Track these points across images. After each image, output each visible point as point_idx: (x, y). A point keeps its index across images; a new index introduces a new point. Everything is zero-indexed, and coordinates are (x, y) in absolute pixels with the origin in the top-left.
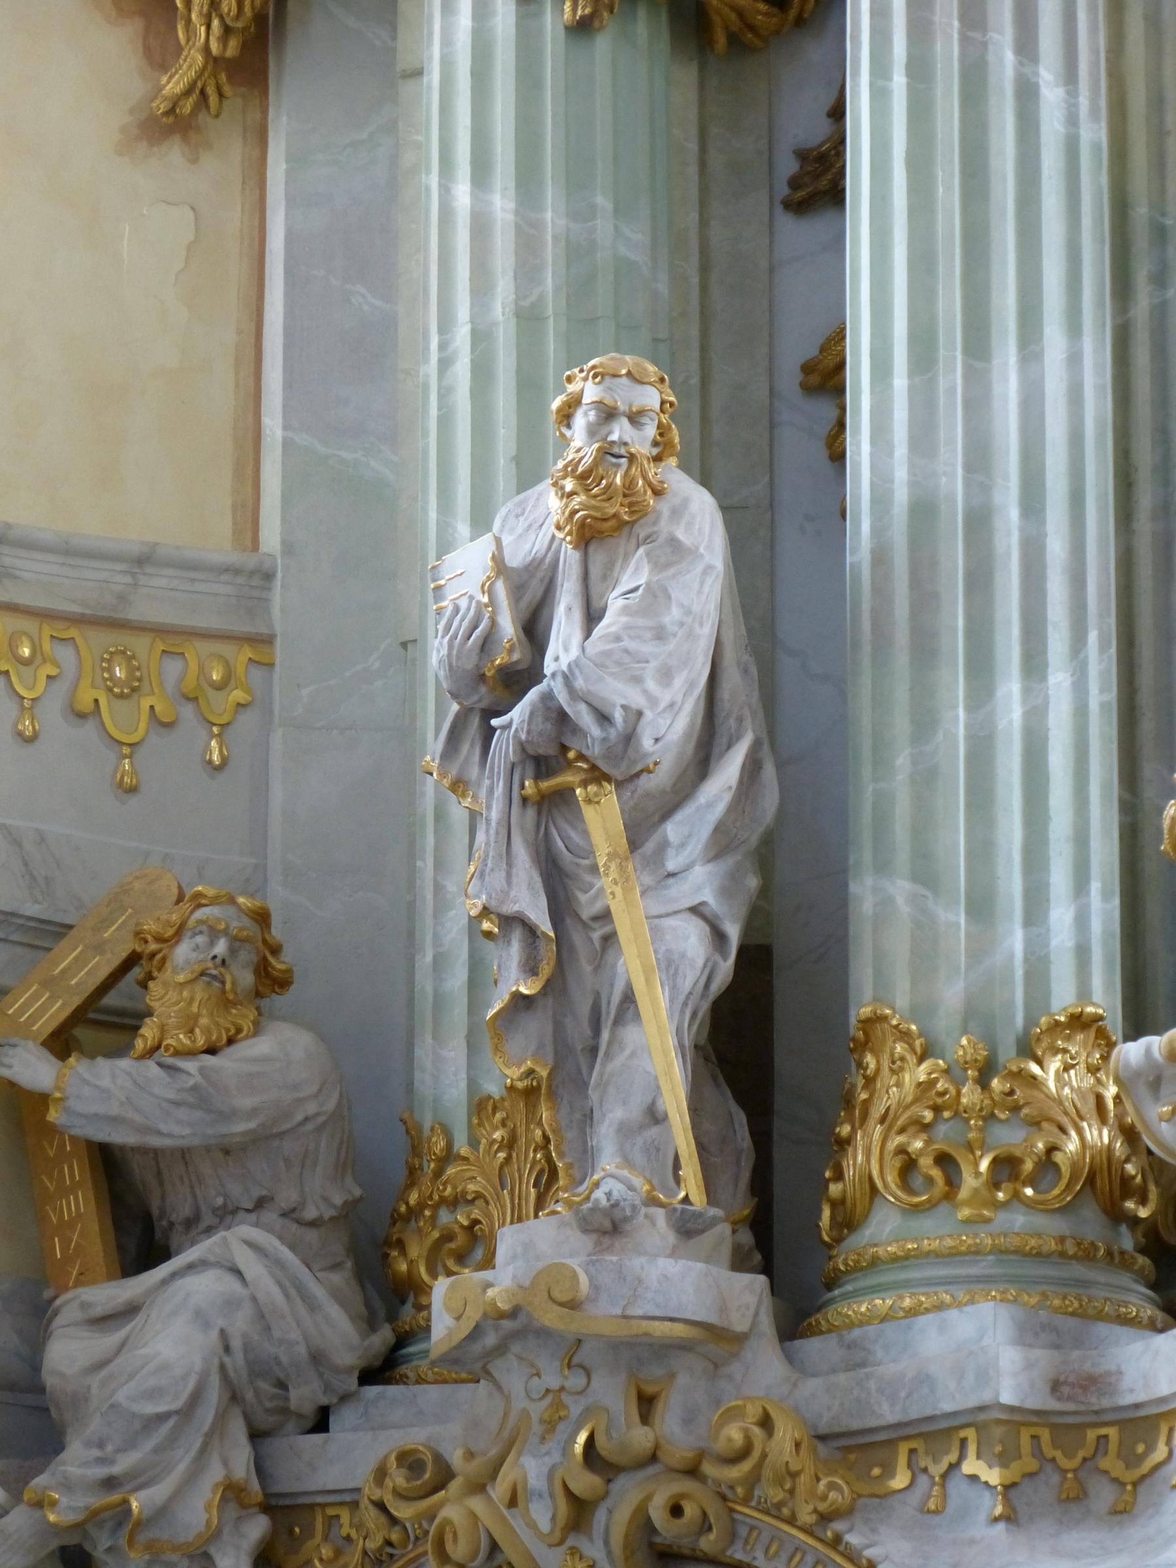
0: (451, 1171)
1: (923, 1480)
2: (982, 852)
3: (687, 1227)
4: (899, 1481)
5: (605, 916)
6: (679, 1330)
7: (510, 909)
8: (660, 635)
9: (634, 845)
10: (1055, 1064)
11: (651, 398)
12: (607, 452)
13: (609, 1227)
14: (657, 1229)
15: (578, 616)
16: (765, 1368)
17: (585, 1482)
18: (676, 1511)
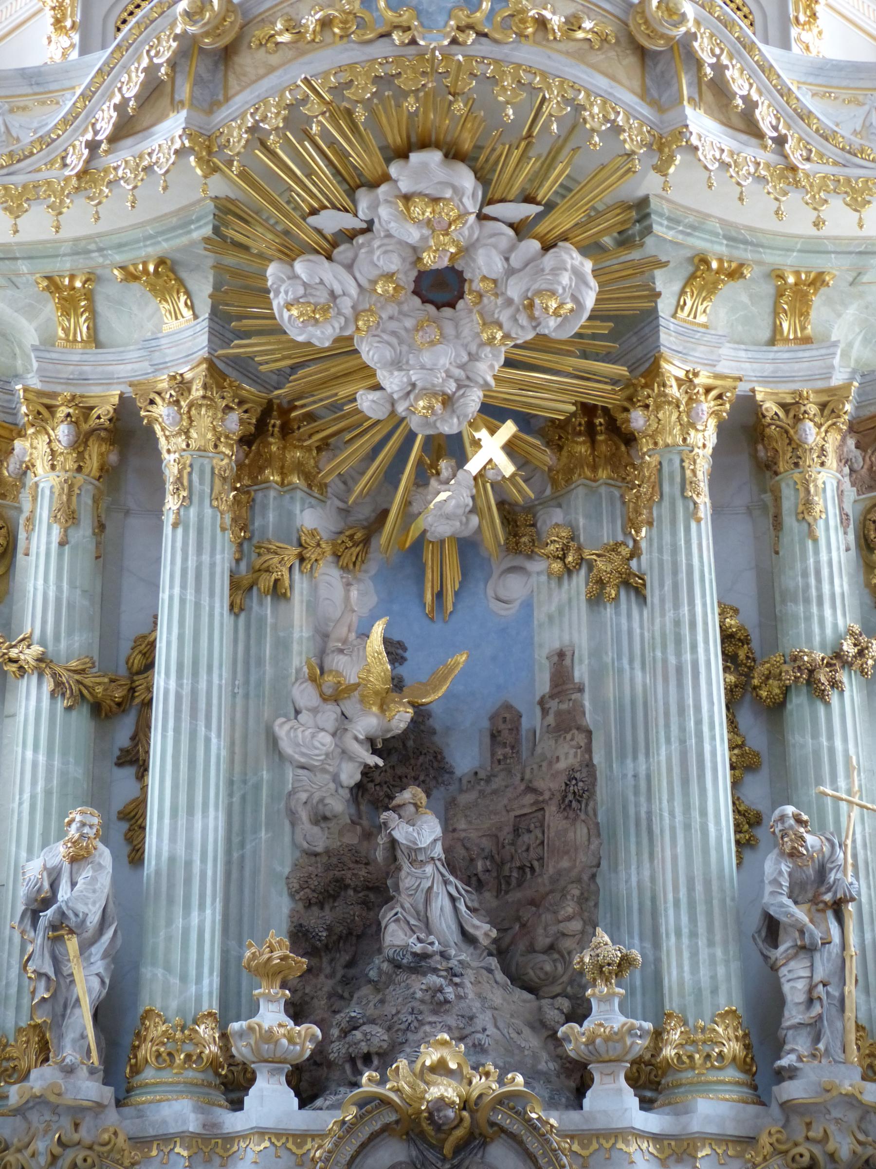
0: (8, 1049)
1: (161, 1154)
2: (185, 961)
3: (92, 1071)
4: (154, 1153)
5: (72, 975)
6: (90, 1104)
7: (42, 971)
8: (94, 891)
9: (81, 954)
10: (203, 1027)
11: (96, 821)
12: (82, 836)
13: (69, 1071)
14: (83, 1072)
15: (69, 884)
16: (112, 1116)
17: (57, 1150)
18: (85, 1160)
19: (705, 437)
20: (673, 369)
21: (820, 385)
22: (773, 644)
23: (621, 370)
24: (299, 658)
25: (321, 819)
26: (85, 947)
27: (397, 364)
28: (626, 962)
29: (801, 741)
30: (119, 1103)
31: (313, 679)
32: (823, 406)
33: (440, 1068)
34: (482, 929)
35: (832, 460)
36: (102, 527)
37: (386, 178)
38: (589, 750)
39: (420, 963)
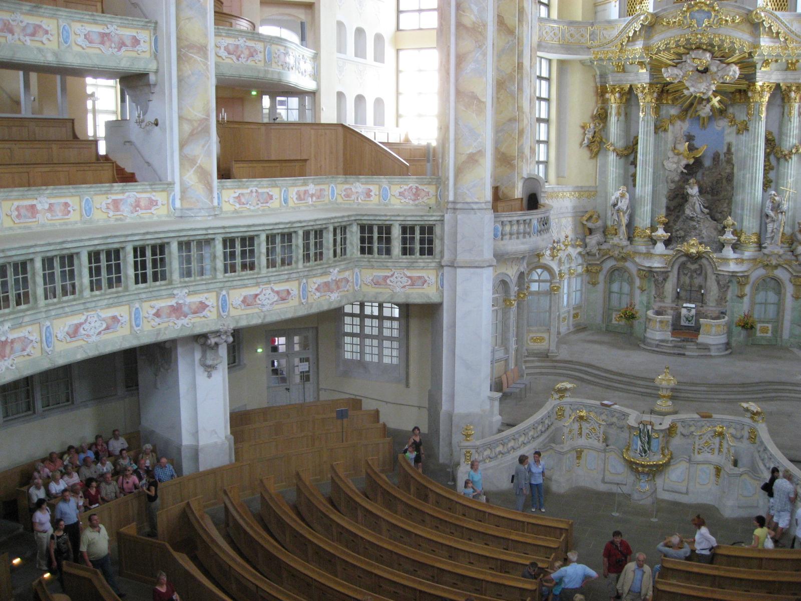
16: (629, 247)
19: (766, 98)
20: (759, 84)
21: (797, 81)
22: (780, 144)
23: (747, 82)
24: (670, 145)
25: (673, 182)
26: (624, 213)
27: (693, 86)
28: (733, 224)
29: (781, 168)
30: (631, 244)
31: (672, 150)
32: (797, 87)
33: (693, 245)
34: (706, 211)
35: (798, 100)
36: (626, 114)
37: (688, 53)
38: (733, 169)
39: (692, 219)
